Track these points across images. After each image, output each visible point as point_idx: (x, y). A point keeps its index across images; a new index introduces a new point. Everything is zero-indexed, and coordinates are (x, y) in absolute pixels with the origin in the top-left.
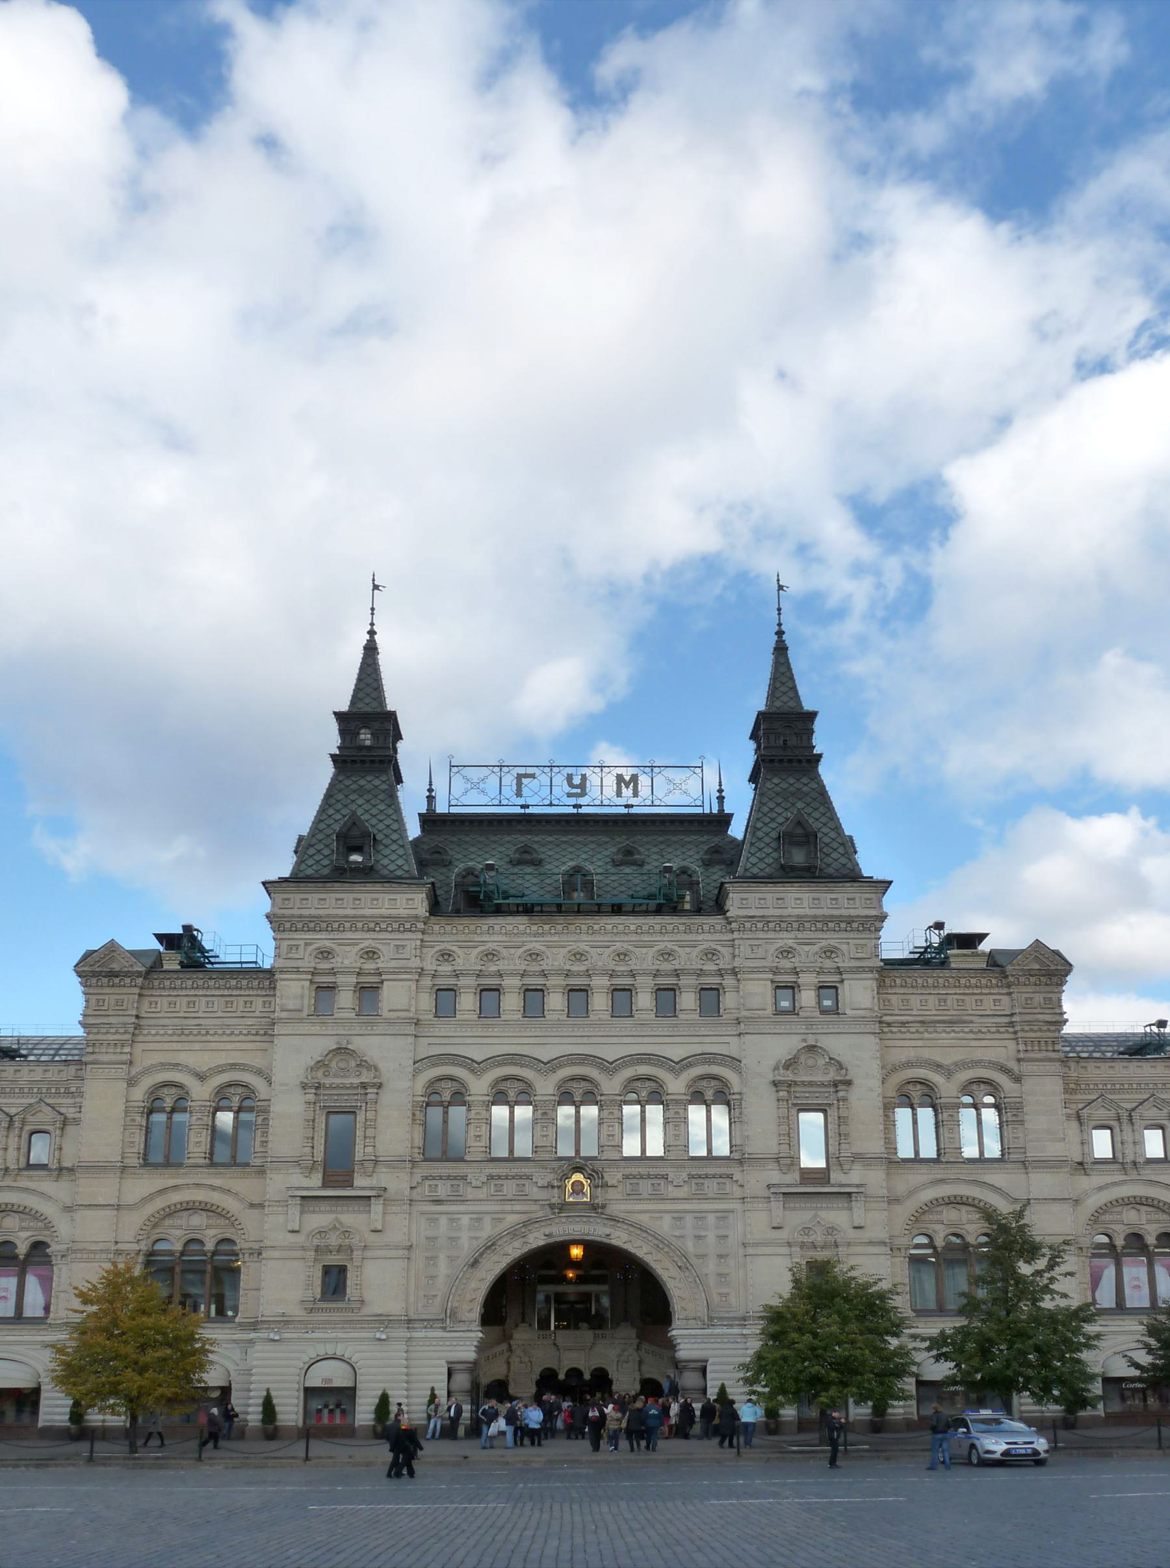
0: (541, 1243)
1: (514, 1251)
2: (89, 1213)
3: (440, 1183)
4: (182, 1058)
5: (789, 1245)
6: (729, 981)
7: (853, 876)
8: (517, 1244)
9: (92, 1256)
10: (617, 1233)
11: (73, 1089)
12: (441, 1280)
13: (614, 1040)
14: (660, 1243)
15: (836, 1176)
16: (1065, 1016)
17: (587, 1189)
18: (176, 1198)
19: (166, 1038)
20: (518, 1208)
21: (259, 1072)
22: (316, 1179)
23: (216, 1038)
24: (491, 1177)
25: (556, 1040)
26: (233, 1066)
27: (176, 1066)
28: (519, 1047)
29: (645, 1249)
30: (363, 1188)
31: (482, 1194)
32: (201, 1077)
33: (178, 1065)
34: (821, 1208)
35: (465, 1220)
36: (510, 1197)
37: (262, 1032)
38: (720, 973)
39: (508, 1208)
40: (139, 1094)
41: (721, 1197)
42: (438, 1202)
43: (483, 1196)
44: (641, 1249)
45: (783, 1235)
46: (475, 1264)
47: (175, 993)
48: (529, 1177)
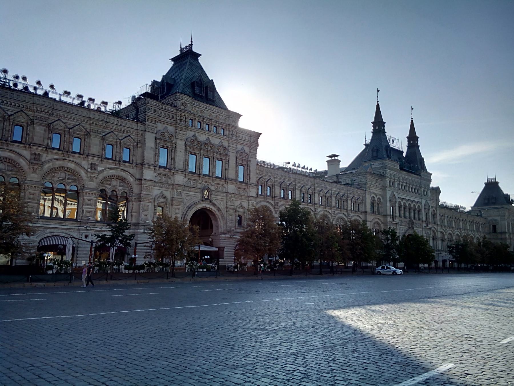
21: (382, 196)
32: (376, 196)
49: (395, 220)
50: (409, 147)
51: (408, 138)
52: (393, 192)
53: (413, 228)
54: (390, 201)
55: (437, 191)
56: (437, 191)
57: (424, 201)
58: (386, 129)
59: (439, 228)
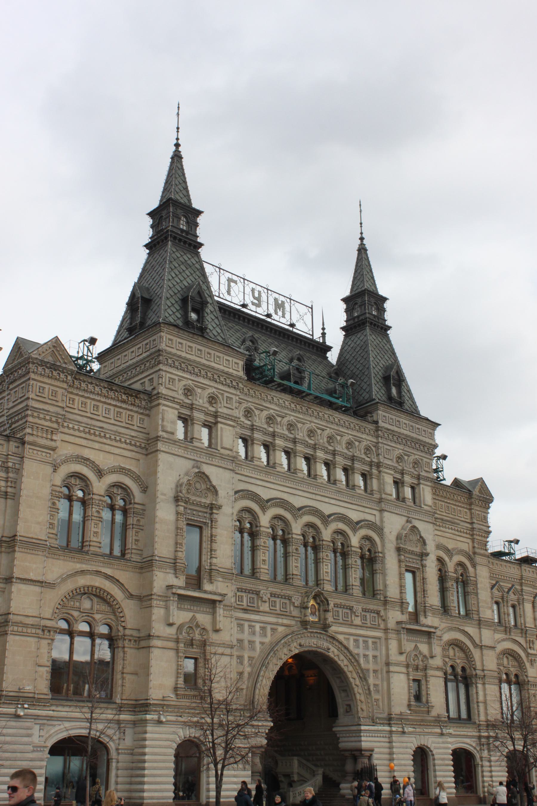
0: (297, 651)
1: (285, 655)
2: (23, 587)
3: (244, 594)
4: (87, 453)
5: (407, 666)
6: (375, 471)
7: (414, 413)
8: (285, 650)
9: (25, 630)
10: (332, 649)
11: (10, 464)
12: (246, 675)
13: (327, 500)
14: (354, 659)
15: (422, 619)
16: (490, 529)
17: (317, 613)
18: (82, 581)
19: (77, 433)
20: (285, 621)
21: (136, 478)
22: (180, 582)
23: (108, 441)
24: (272, 595)
25: (300, 493)
26: (122, 470)
27: (86, 461)
28: (283, 493)
29: (346, 662)
30: (206, 592)
31: (265, 607)
32: (100, 473)
33: (88, 459)
34: (416, 641)
35: (258, 627)
36: (279, 612)
37: (138, 444)
38: (371, 464)
39: (280, 621)
40: (58, 478)
41: (374, 628)
42: (245, 611)
43: (267, 609)
44: (343, 662)
45: (403, 658)
46: (264, 664)
47: (86, 395)
48: (289, 598)
49: (207, 587)
50: (349, 330)
51: (345, 300)
52: (197, 464)
53: (325, 627)
54: (177, 499)
55: (474, 496)
56: (474, 496)
57: (394, 524)
58: (203, 233)
59: (488, 636)
